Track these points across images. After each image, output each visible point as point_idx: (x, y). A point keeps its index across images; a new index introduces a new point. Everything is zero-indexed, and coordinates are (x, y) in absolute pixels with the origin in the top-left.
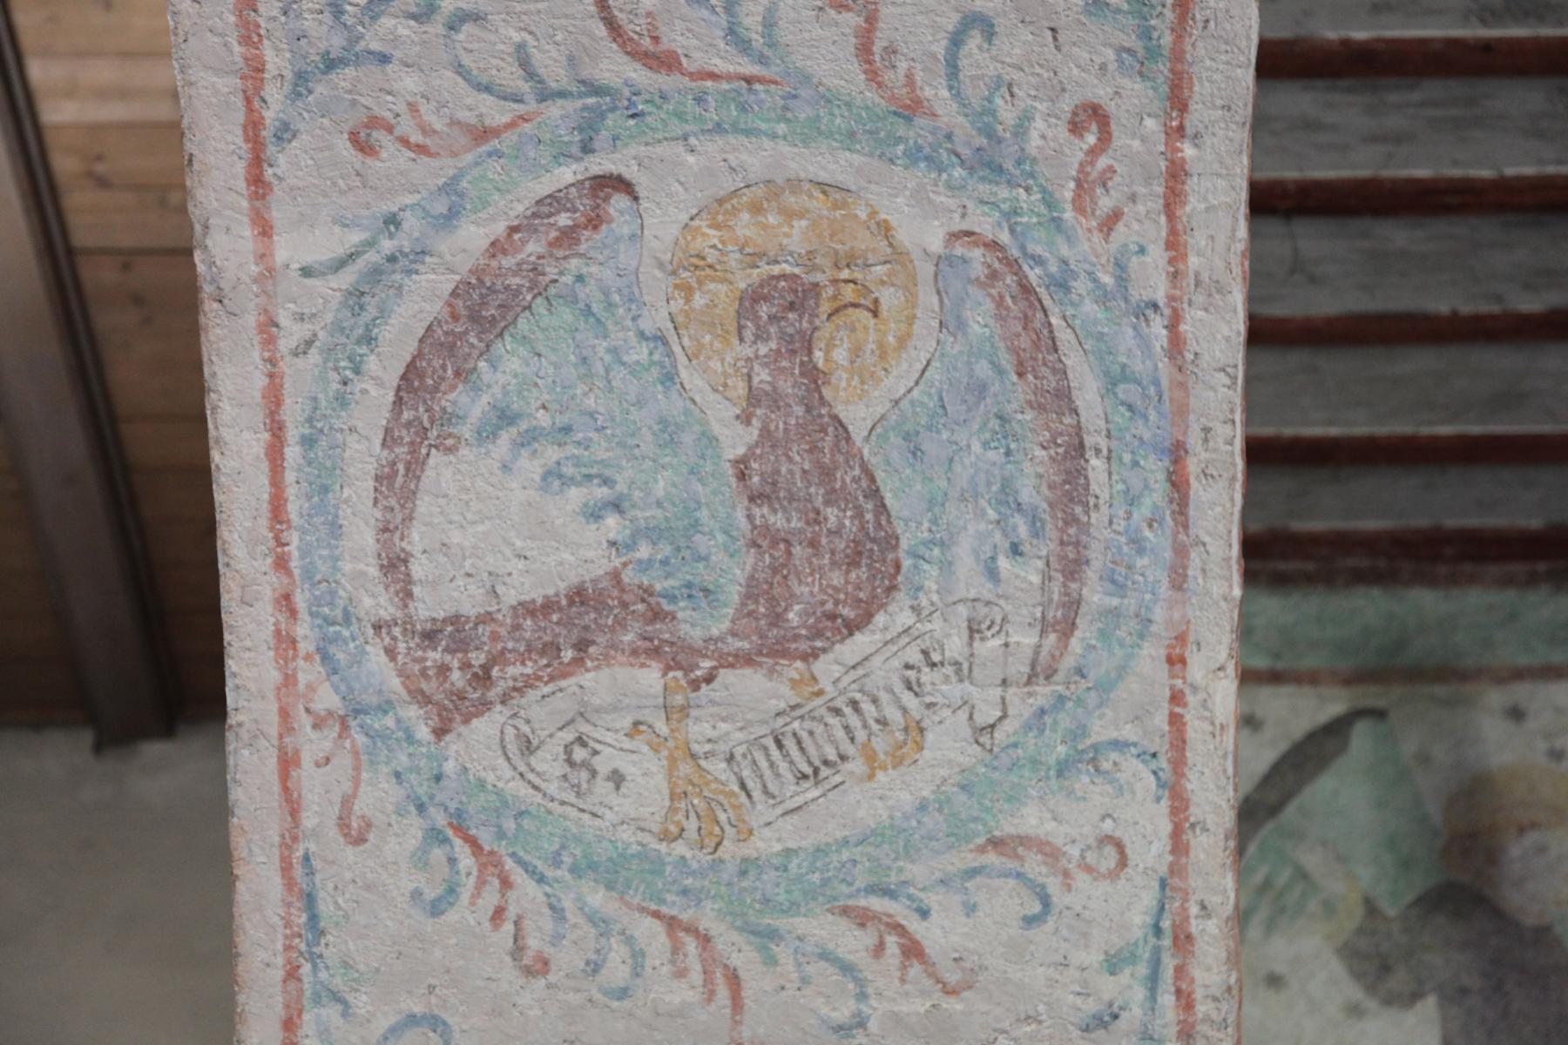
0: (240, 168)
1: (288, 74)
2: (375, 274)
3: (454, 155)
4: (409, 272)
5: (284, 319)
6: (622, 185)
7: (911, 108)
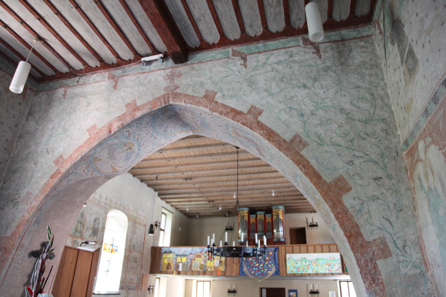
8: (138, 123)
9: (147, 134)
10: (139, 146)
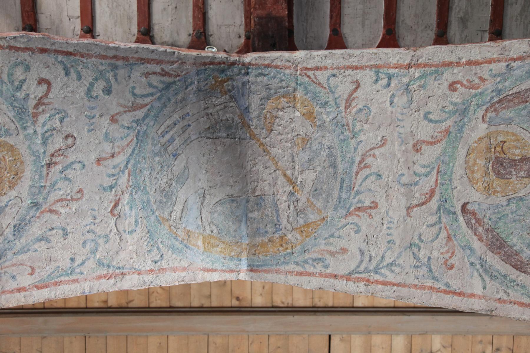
0: (456, 297)
1: (433, 281)
2: (486, 271)
3: (455, 246)
4: (486, 262)
5: (499, 297)
6: (464, 206)
7: (447, 132)
8: (101, 75)
9: (98, 161)
10: (36, 205)
